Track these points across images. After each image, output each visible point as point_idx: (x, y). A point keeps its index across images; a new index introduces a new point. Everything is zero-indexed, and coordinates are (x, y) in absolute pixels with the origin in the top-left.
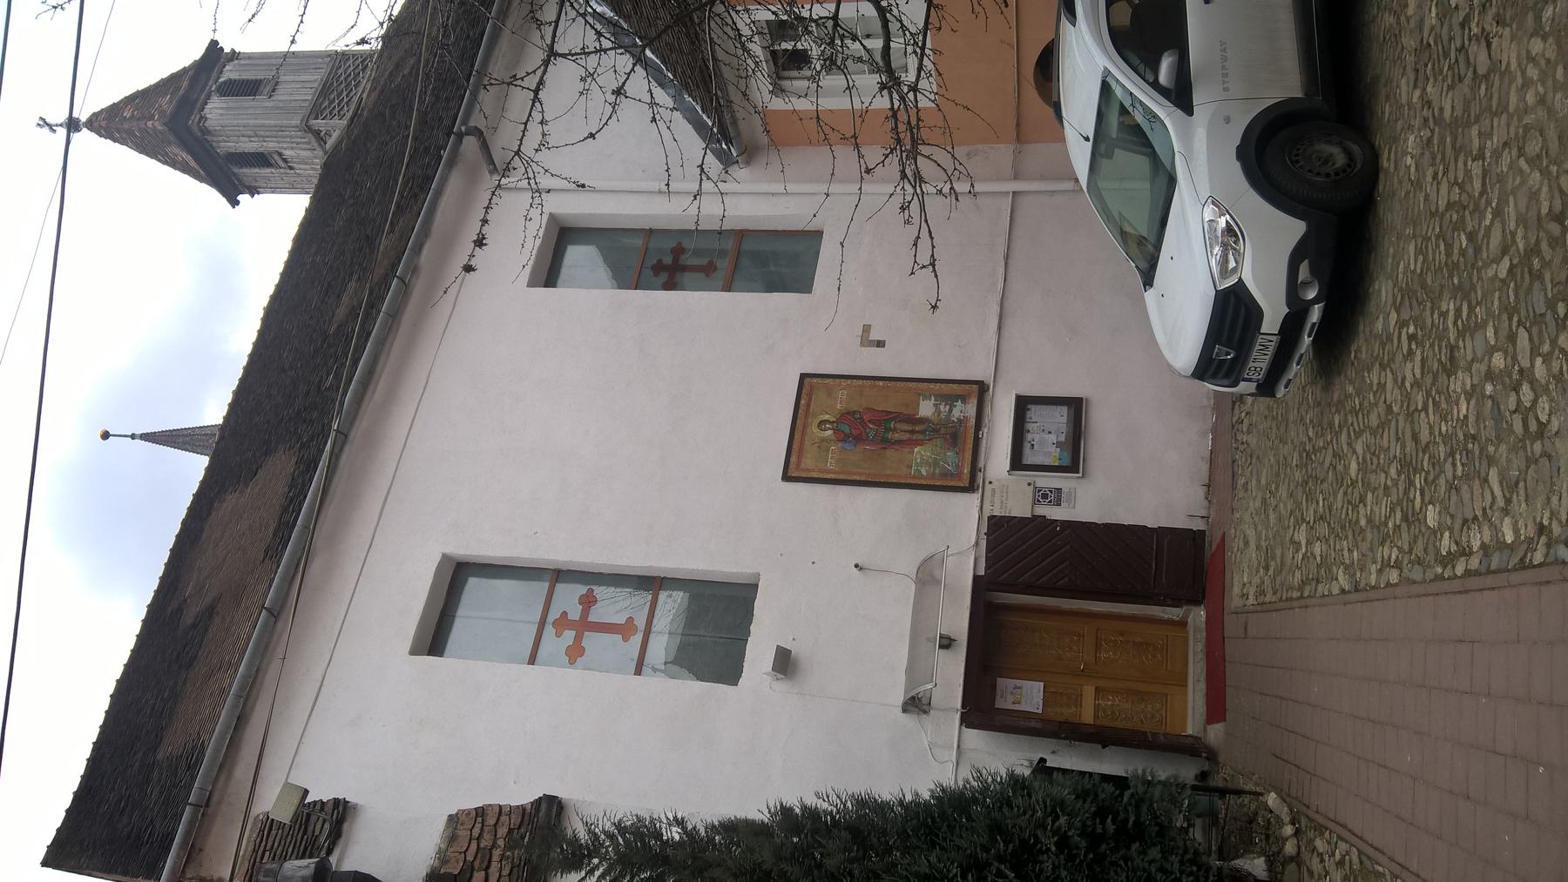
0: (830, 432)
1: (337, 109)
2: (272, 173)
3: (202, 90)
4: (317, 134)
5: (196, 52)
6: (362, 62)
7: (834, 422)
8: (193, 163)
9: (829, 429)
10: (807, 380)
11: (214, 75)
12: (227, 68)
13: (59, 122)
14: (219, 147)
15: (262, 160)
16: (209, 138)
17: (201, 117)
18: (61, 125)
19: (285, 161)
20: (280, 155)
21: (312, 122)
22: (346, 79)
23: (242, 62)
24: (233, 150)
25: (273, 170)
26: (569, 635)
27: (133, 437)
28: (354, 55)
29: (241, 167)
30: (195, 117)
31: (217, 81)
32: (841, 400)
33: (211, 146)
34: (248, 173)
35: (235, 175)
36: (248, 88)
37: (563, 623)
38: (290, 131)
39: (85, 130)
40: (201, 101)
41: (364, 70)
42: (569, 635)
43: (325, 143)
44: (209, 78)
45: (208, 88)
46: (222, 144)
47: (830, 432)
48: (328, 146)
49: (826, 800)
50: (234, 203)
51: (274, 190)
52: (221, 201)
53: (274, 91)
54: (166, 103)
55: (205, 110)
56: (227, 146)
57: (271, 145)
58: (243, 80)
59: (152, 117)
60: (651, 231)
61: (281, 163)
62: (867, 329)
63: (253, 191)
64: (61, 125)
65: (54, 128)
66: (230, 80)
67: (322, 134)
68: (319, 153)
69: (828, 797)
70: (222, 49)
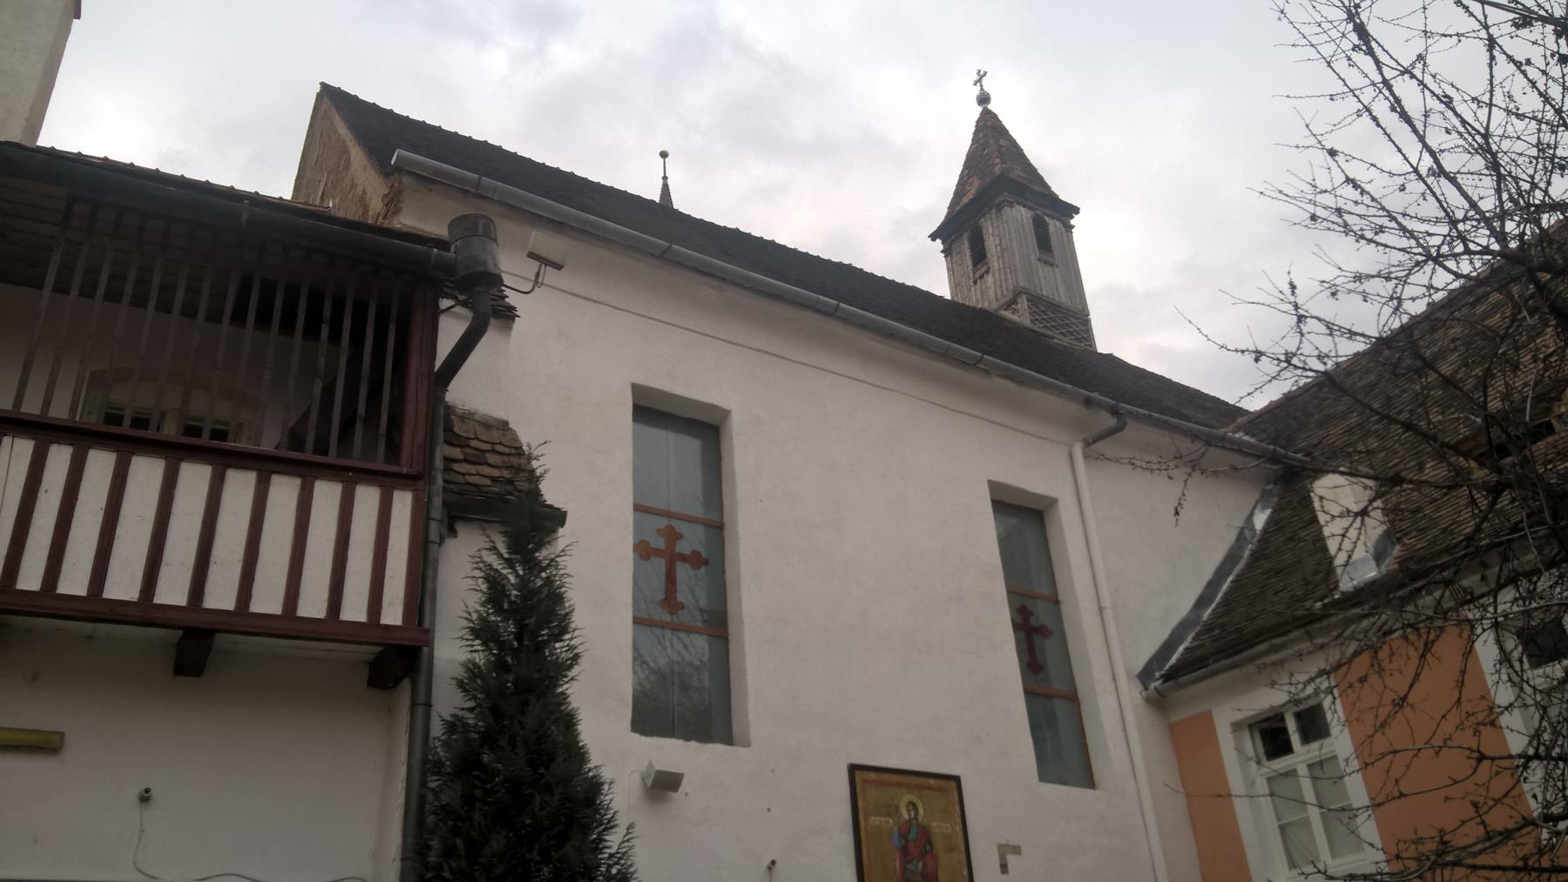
0: (906, 816)
2: (967, 267)
4: (1014, 301)
6: (1083, 338)
7: (917, 819)
8: (965, 200)
9: (910, 815)
10: (953, 784)
11: (1049, 212)
12: (1058, 223)
13: (984, 88)
14: (985, 220)
15: (979, 256)
16: (994, 211)
18: (982, 89)
19: (982, 276)
20: (987, 272)
21: (1024, 298)
24: (984, 231)
25: (970, 267)
26: (660, 543)
29: (969, 241)
31: (1043, 214)
32: (939, 827)
33: (986, 213)
35: (961, 235)
36: (1044, 242)
37: (673, 536)
38: (1012, 279)
40: (1025, 202)
41: (1077, 339)
42: (660, 543)
43: (1006, 310)
47: (906, 816)
49: (626, 838)
50: (933, 237)
51: (950, 270)
54: (1017, 173)
55: (1018, 207)
56: (989, 228)
57: (996, 264)
59: (1004, 162)
60: (1057, 602)
61: (979, 273)
62: (1016, 850)
63: (947, 252)
64: (982, 89)
65: (978, 84)
67: (1014, 306)
69: (628, 841)
70: (1073, 217)
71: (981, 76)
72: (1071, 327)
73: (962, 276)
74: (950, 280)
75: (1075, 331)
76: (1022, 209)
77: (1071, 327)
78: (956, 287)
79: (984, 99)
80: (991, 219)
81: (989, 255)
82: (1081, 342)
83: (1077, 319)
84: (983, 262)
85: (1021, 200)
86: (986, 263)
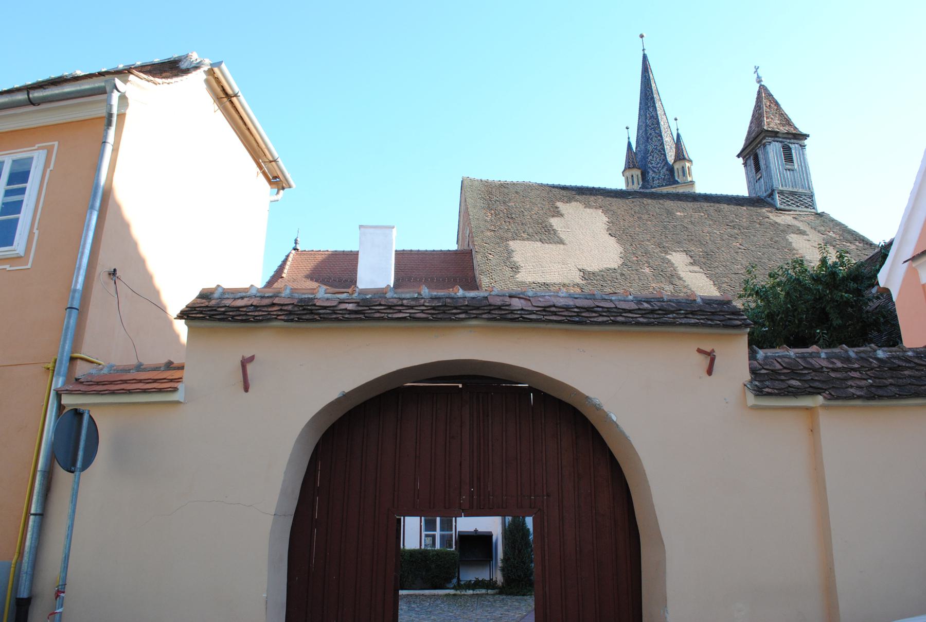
1: (784, 201)
5: (804, 131)
6: (810, 205)
12: (797, 145)
15: (758, 168)
17: (770, 142)
22: (800, 200)
23: (801, 151)
27: (629, 138)
28: (812, 200)
29: (753, 160)
30: (770, 139)
31: (789, 143)
33: (760, 147)
34: (751, 162)
35: (750, 157)
39: (759, 85)
41: (806, 207)
44: (790, 139)
48: (768, 199)
50: (738, 156)
51: (747, 174)
52: (739, 152)
53: (789, 170)
57: (764, 173)
58: (792, 155)
59: (767, 118)
63: (745, 164)
66: (791, 149)
67: (772, 196)
68: (765, 195)
70: (806, 139)
71: (757, 68)
72: (802, 201)
77: (802, 201)
78: (749, 182)
79: (759, 80)
85: (776, 139)
86: (761, 173)
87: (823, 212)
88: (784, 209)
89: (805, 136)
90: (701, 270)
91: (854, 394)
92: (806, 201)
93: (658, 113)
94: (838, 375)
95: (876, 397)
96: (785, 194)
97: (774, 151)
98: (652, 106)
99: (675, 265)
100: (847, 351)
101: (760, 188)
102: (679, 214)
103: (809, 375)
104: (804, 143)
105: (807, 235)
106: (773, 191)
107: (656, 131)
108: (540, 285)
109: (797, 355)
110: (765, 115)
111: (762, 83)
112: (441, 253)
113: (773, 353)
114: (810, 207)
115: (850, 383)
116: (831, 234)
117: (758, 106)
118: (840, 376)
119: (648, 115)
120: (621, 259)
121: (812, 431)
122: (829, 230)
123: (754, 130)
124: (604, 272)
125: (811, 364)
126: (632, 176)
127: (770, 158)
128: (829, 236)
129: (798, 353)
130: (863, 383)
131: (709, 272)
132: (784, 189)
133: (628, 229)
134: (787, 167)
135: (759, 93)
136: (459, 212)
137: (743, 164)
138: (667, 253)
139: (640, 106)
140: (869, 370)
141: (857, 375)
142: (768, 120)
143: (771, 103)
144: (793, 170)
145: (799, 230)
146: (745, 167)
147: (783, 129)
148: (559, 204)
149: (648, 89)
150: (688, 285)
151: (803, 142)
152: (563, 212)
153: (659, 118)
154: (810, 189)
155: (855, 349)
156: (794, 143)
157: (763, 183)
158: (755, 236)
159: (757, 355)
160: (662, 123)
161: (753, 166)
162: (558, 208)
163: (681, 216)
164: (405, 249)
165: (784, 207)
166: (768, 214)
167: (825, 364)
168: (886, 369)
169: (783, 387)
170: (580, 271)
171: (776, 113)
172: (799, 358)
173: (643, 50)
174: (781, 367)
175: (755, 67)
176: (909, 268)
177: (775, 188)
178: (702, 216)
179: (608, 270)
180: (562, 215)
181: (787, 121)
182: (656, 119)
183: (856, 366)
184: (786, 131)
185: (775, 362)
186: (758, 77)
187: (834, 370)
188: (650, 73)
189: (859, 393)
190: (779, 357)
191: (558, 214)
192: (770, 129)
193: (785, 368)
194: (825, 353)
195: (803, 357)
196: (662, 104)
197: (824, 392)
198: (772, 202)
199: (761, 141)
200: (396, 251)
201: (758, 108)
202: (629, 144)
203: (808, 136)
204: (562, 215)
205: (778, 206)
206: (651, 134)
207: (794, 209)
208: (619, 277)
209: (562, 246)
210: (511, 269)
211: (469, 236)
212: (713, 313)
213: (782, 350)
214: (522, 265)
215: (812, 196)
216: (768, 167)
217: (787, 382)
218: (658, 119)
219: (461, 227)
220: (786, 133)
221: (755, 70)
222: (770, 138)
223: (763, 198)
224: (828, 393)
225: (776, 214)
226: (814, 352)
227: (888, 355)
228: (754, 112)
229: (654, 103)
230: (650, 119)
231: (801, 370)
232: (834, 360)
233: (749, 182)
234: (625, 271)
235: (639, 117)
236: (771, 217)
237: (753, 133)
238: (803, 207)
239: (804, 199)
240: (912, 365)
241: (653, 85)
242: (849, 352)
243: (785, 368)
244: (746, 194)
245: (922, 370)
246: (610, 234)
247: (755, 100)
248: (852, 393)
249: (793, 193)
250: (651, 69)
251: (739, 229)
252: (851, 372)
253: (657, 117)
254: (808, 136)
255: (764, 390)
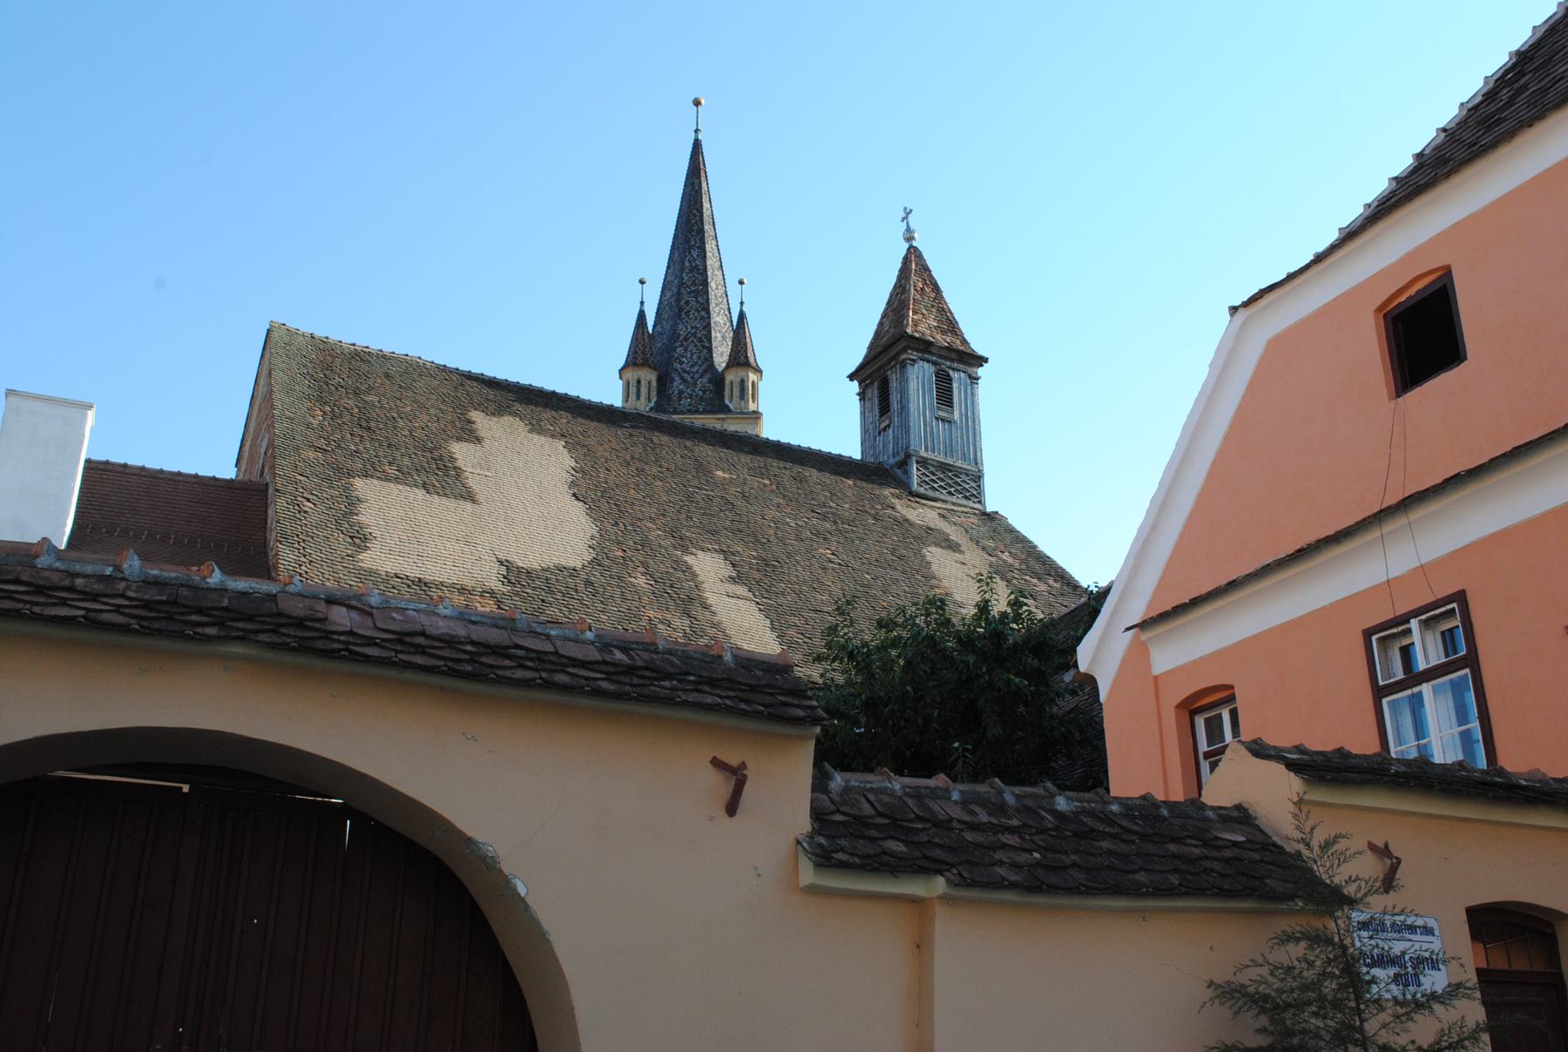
1: (927, 479)
3: (940, 357)
5: (978, 347)
6: (973, 495)
11: (955, 365)
12: (962, 375)
15: (885, 408)
17: (914, 361)
19: (885, 429)
20: (889, 426)
22: (956, 483)
23: (969, 387)
24: (891, 385)
25: (877, 417)
27: (642, 303)
28: (979, 486)
29: (878, 389)
30: (914, 355)
31: (950, 368)
34: (874, 392)
35: (872, 383)
39: (907, 246)
41: (966, 497)
43: (898, 468)
44: (952, 360)
45: (943, 361)
46: (894, 375)
48: (896, 470)
50: (852, 377)
51: (863, 414)
52: (852, 369)
53: (943, 420)
57: (896, 419)
59: (915, 312)
61: (883, 426)
63: (862, 395)
66: (951, 380)
68: (892, 461)
70: (982, 365)
71: (908, 213)
72: (960, 485)
73: (872, 423)
74: (861, 424)
75: (965, 488)
76: (926, 365)
79: (909, 236)
80: (896, 373)
81: (892, 409)
82: (970, 500)
83: (967, 475)
84: (886, 415)
87: (997, 513)
88: (923, 494)
89: (981, 361)
90: (750, 595)
91: (1004, 879)
92: (967, 486)
93: (709, 262)
94: (979, 838)
95: (1045, 887)
96: (929, 466)
97: (918, 378)
98: (698, 247)
99: (700, 579)
100: (1000, 792)
101: (884, 446)
102: (720, 473)
103: (925, 832)
104: (977, 373)
105: (962, 552)
106: (908, 456)
107: (700, 299)
108: (410, 583)
109: (907, 790)
110: (911, 306)
111: (914, 244)
112: (193, 480)
113: (861, 782)
114: (972, 498)
115: (999, 855)
116: (1006, 556)
117: (900, 286)
118: (983, 840)
119: (687, 264)
120: (591, 550)
121: (918, 946)
122: (1002, 548)
123: (887, 331)
124: (552, 573)
125: (930, 810)
126: (639, 382)
127: (911, 392)
128: (1001, 559)
129: (908, 787)
130: (1022, 858)
131: (764, 600)
132: (929, 455)
133: (613, 490)
134: (941, 413)
135: (906, 261)
136: (252, 397)
137: (859, 394)
138: (685, 550)
139: (673, 242)
140: (1037, 833)
141: (1012, 840)
142: (915, 317)
143: (926, 284)
144: (950, 422)
145: (947, 540)
146: (860, 400)
147: (942, 340)
148: (475, 415)
149: (695, 211)
150: (720, 623)
151: (975, 370)
152: (482, 433)
153: (709, 274)
154: (977, 464)
155: (1017, 790)
156: (959, 370)
157: (891, 437)
158: (862, 540)
159: (830, 782)
160: (713, 285)
161: (876, 400)
162: (473, 423)
163: (724, 478)
164: (111, 460)
165: (925, 492)
166: (893, 500)
167: (957, 813)
168: (1069, 834)
169: (872, 852)
170: (501, 563)
171: (933, 306)
172: (907, 795)
173: (697, 131)
174: (873, 813)
175: (906, 208)
176: (1136, 639)
177: (911, 452)
178: (765, 485)
179: (561, 569)
180: (479, 440)
181: (951, 326)
182: (702, 274)
183: (1015, 822)
184: (946, 344)
185: (863, 800)
186: (908, 230)
187: (972, 827)
188: (703, 179)
189: (1013, 877)
190: (871, 790)
191: (472, 437)
192: (917, 335)
193: (880, 814)
194: (961, 791)
195: (917, 795)
196: (717, 246)
197: (948, 870)
198: (903, 477)
199: (898, 354)
200: (88, 461)
201: (900, 290)
202: (642, 316)
203: (986, 360)
204: (479, 440)
205: (915, 487)
206: (687, 303)
207: (943, 497)
208: (581, 587)
209: (468, 506)
210: (350, 540)
211: (265, 453)
212: (753, 688)
213: (879, 778)
214: (376, 533)
215: (979, 477)
216: (904, 408)
217: (881, 843)
218: (707, 275)
219: (251, 430)
220: (947, 348)
221: (903, 215)
222: (914, 353)
223: (888, 467)
224: (955, 871)
225: (909, 503)
226: (940, 788)
227: (1075, 806)
228: (891, 295)
229: (703, 243)
230: (691, 271)
231: (911, 821)
232: (977, 809)
233: (865, 431)
234: (596, 577)
235: (668, 263)
236: (899, 507)
237: (884, 336)
238: (960, 496)
239: (963, 481)
240: (1116, 830)
241: (706, 205)
242: (1005, 795)
243: (880, 814)
244: (857, 455)
245: (1133, 842)
246: (574, 495)
247: (897, 273)
248: (1001, 875)
249: (944, 467)
250: (706, 172)
251: (835, 522)
252: (1003, 834)
253: (706, 271)
254: (986, 360)
255: (835, 855)
